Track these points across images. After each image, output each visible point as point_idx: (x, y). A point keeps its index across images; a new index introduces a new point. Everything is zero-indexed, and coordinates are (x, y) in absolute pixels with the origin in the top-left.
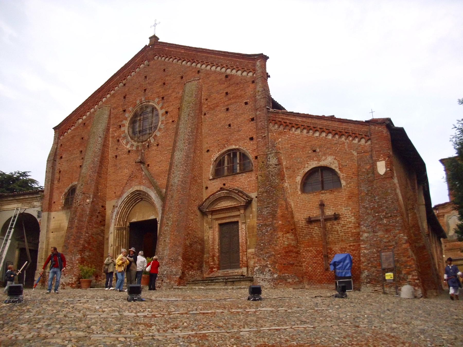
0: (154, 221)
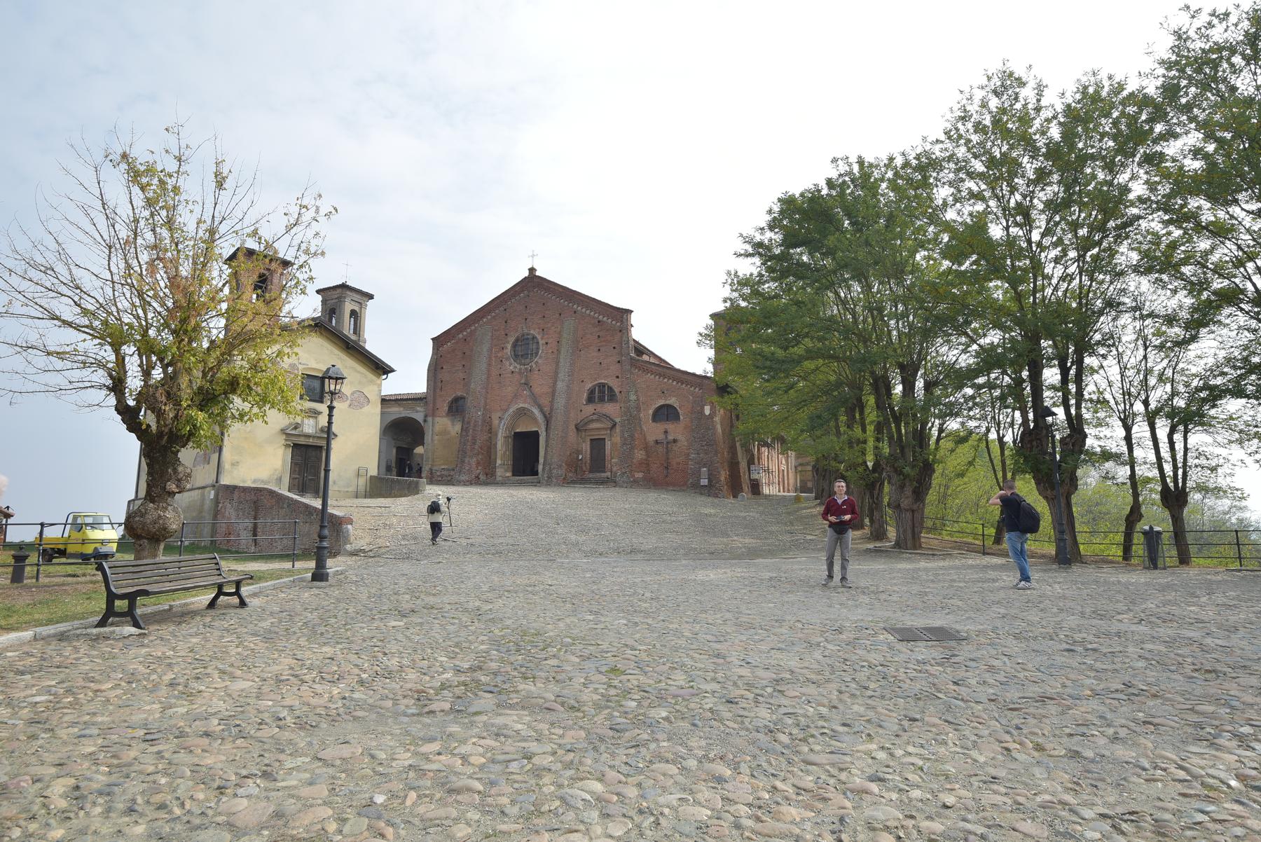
0: (535, 435)
